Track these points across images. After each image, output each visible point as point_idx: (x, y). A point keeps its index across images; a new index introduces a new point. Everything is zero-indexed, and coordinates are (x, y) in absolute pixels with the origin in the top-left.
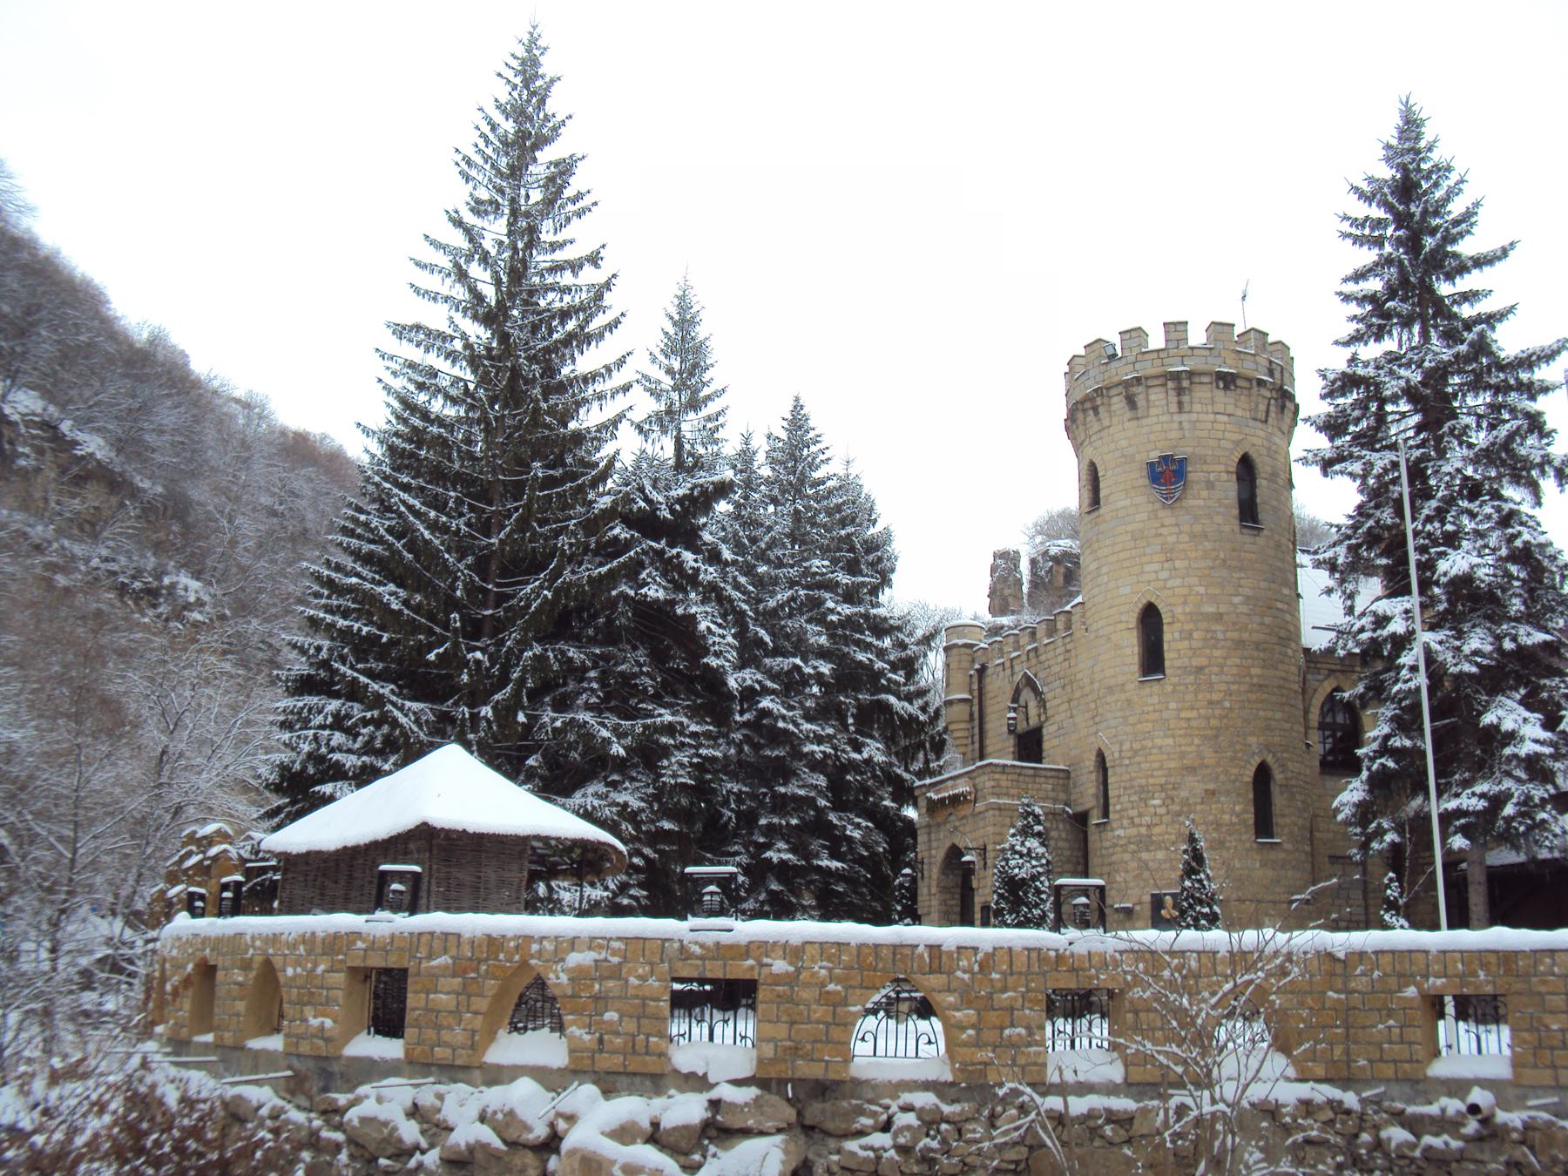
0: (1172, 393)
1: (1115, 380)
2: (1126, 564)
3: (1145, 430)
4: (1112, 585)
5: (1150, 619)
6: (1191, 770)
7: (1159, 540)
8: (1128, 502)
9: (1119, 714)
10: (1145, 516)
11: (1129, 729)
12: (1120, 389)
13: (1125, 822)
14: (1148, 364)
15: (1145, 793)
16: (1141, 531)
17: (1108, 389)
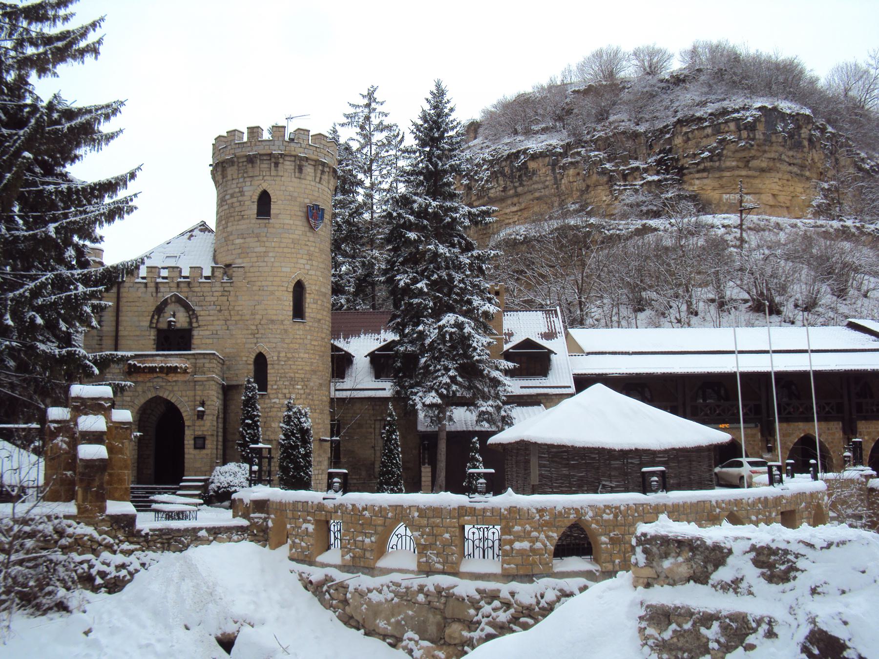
0: (319, 172)
1: (293, 153)
2: (288, 255)
3: (303, 186)
4: (276, 264)
5: (299, 289)
6: (314, 372)
7: (307, 248)
8: (291, 222)
9: (278, 336)
10: (300, 233)
11: (285, 346)
12: (293, 159)
13: (280, 396)
14: (311, 152)
15: (293, 381)
16: (299, 240)
17: (286, 155)
